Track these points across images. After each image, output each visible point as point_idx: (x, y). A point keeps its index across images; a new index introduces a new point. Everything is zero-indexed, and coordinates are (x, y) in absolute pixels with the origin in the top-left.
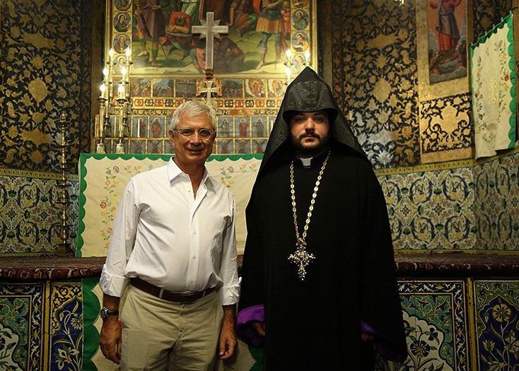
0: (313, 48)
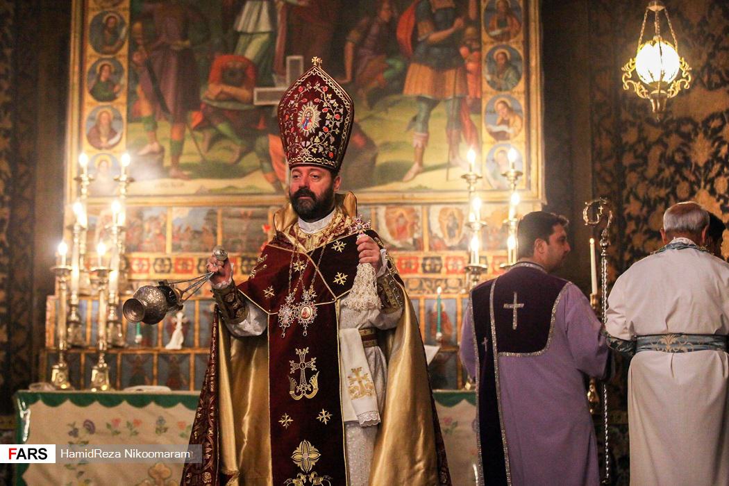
0: (533, 132)
